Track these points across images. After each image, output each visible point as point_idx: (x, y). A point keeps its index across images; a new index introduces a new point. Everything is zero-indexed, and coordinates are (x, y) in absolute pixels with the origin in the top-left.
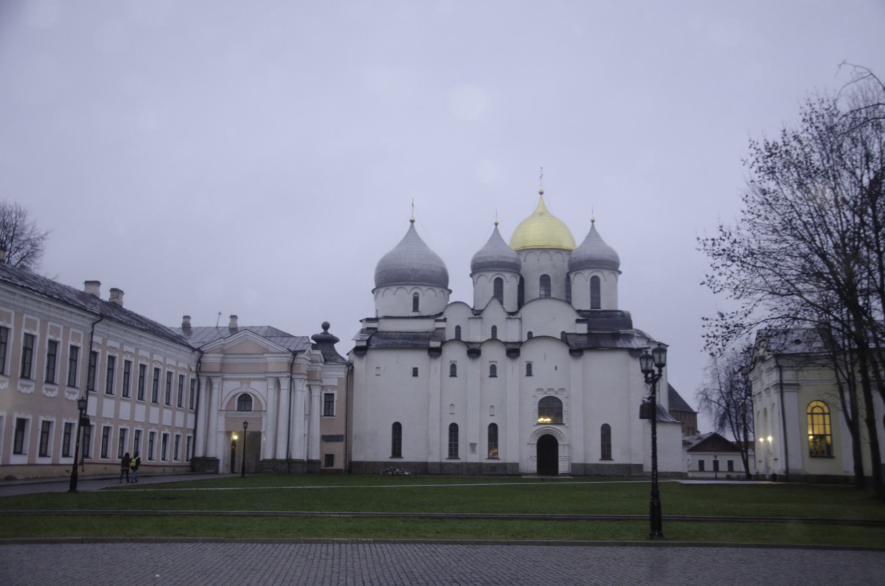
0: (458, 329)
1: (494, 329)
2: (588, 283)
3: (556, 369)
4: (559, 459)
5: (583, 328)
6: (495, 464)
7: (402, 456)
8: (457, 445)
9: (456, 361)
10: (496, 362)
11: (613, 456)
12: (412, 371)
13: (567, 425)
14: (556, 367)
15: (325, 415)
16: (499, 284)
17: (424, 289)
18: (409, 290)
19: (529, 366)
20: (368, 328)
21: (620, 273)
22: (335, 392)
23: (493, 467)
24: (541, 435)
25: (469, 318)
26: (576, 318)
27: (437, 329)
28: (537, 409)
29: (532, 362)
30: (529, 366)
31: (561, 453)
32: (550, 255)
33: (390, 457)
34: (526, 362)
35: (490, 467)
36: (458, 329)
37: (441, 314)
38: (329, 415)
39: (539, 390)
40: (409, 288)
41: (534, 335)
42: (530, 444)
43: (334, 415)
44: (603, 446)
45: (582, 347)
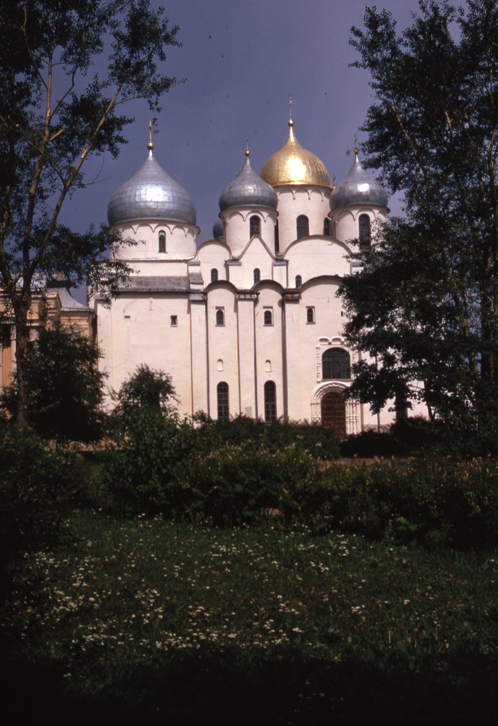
0: (214, 272)
4: (347, 420)
9: (223, 308)
10: (272, 307)
12: (170, 320)
16: (255, 223)
17: (172, 226)
18: (153, 228)
19: (310, 311)
24: (324, 393)
28: (321, 362)
29: (314, 307)
30: (310, 311)
32: (308, 193)
34: (307, 307)
36: (214, 272)
39: (322, 340)
40: (153, 226)
41: (304, 281)
42: (314, 404)
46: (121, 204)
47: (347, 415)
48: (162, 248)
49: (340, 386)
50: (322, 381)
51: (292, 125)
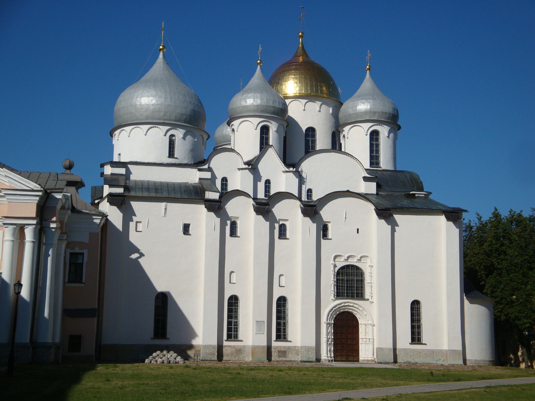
0: (224, 180)
1: (268, 182)
2: (368, 137)
3: (358, 233)
4: (360, 342)
5: (371, 188)
6: (284, 347)
7: (168, 336)
8: (236, 324)
11: (424, 339)
13: (370, 300)
14: (358, 230)
15: (69, 282)
20: (112, 174)
21: (399, 128)
22: (85, 252)
23: (283, 353)
25: (239, 169)
26: (364, 176)
27: (200, 179)
29: (329, 222)
31: (361, 335)
33: (152, 338)
35: (279, 352)
37: (203, 162)
38: (75, 282)
43: (83, 281)
44: (413, 327)
45: (389, 207)
46: (131, 105)
47: (360, 337)
48: (171, 154)
49: (355, 305)
50: (336, 299)
51: (302, 36)
